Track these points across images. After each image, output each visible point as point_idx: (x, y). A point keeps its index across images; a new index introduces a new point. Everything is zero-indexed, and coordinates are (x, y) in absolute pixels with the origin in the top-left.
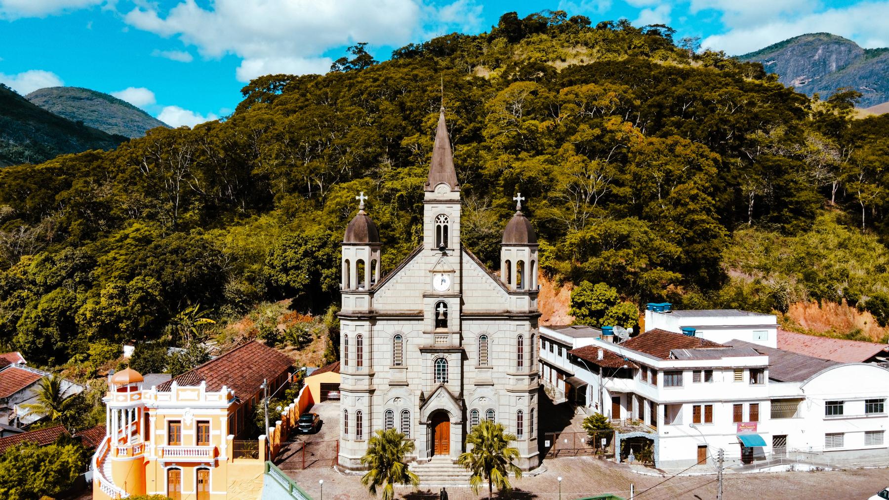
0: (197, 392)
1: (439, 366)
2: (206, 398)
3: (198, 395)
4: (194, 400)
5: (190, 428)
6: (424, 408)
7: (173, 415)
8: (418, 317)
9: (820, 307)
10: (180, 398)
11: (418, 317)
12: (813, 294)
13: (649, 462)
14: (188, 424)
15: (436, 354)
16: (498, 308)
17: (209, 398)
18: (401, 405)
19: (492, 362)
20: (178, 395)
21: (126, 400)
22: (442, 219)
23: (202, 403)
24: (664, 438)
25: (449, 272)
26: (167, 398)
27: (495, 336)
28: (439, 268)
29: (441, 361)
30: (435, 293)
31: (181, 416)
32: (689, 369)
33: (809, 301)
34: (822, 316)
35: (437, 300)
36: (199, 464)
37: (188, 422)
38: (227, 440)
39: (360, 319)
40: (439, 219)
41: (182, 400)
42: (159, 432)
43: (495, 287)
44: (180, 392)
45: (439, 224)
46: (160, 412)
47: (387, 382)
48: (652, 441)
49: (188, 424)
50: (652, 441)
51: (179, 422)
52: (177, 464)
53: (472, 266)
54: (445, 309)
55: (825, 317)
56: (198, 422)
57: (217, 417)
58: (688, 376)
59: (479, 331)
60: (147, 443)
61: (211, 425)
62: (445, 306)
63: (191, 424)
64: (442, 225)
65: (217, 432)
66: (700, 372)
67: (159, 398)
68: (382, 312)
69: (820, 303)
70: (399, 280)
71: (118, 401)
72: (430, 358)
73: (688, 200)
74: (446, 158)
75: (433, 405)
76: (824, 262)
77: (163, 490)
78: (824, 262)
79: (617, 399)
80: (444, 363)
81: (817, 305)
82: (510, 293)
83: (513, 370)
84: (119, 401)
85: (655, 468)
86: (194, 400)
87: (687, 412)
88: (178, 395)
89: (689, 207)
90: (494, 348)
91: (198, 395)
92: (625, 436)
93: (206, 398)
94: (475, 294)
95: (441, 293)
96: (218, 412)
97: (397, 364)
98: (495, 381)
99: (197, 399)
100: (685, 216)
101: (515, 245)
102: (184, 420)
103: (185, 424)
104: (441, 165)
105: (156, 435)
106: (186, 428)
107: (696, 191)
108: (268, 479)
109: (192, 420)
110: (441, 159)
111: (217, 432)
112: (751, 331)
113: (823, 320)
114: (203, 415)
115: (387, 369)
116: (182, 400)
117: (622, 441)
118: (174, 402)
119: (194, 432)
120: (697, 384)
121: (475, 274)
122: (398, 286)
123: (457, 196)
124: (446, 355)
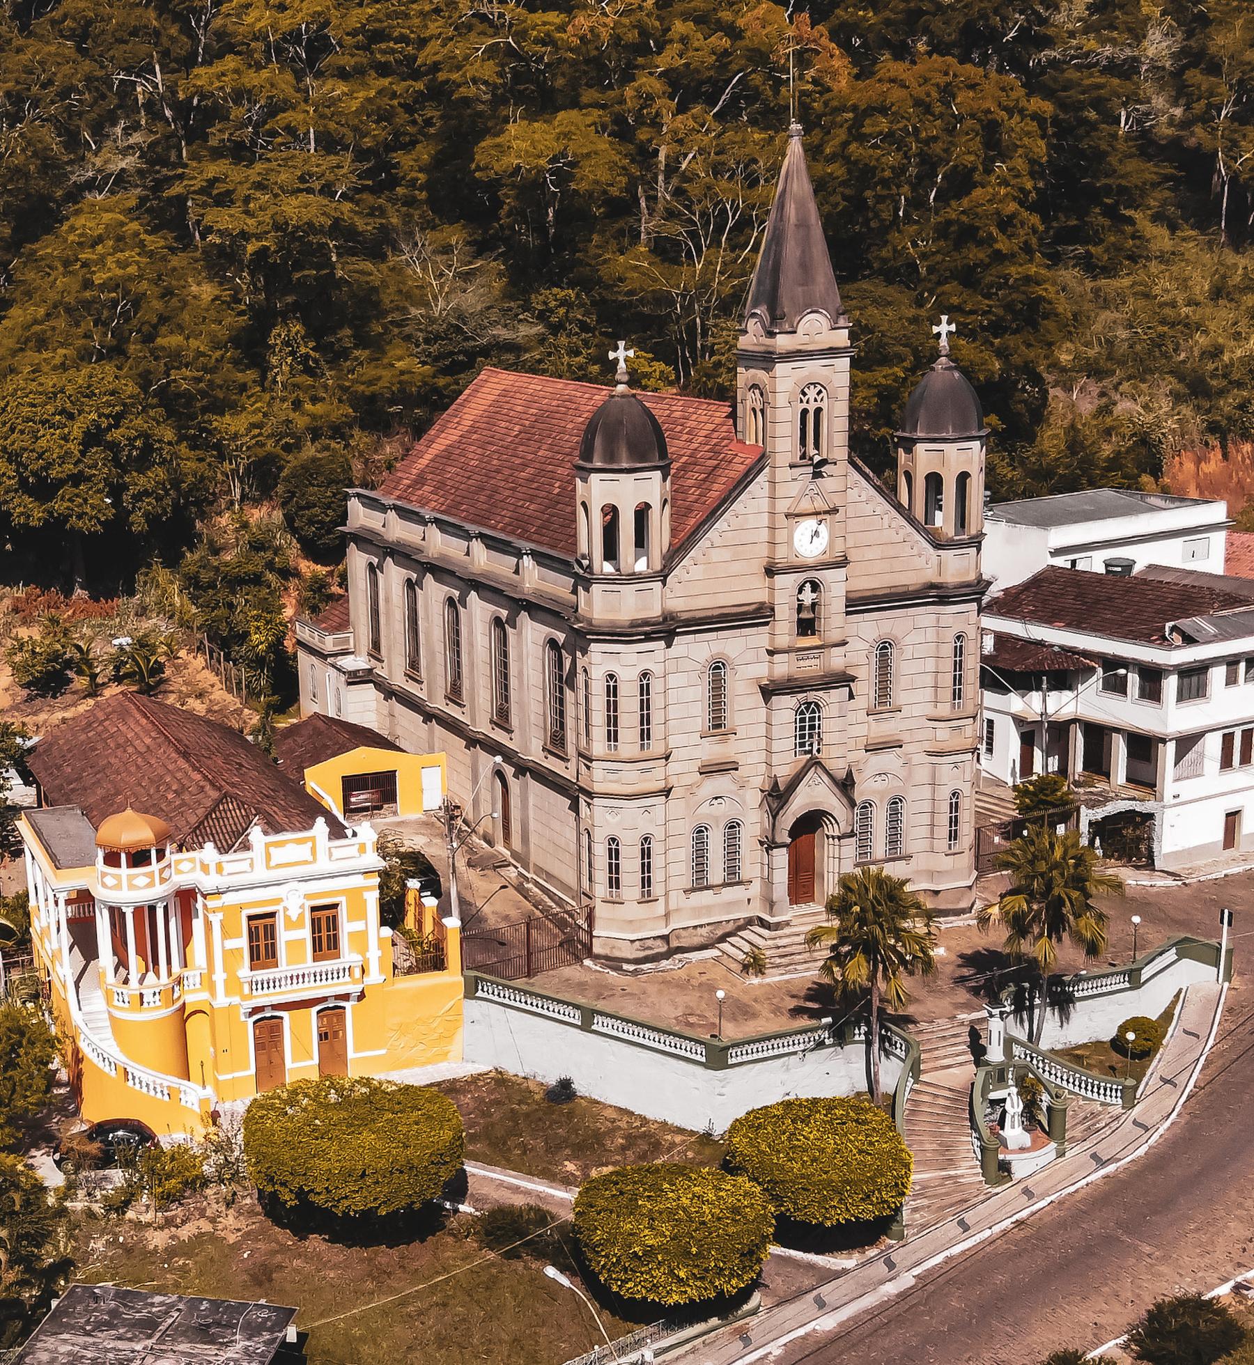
0: (310, 844)
1: (803, 720)
2: (330, 855)
3: (313, 851)
4: (306, 862)
5: (298, 925)
6: (781, 813)
7: (256, 901)
8: (760, 615)
9: (1225, 456)
10: (272, 864)
11: (760, 615)
12: (1213, 428)
13: (1139, 859)
14: (294, 918)
15: (800, 696)
16: (912, 579)
17: (337, 853)
18: (724, 811)
19: (900, 696)
20: (268, 856)
21: (151, 885)
22: (812, 393)
23: (324, 865)
24: (1175, 805)
25: (826, 512)
26: (244, 866)
27: (908, 640)
28: (805, 506)
29: (807, 709)
30: (796, 561)
31: (278, 901)
32: (1215, 661)
33: (1207, 444)
34: (1231, 477)
35: (801, 577)
36: (325, 999)
37: (294, 914)
38: (379, 939)
39: (649, 638)
40: (804, 394)
41: (279, 866)
42: (231, 944)
43: (909, 535)
44: (272, 850)
45: (805, 405)
46: (229, 899)
47: (695, 766)
48: (1151, 816)
49: (294, 918)
50: (1151, 816)
51: (272, 915)
52: (275, 1007)
53: (864, 494)
54: (814, 595)
55: (1235, 479)
56: (314, 909)
57: (355, 895)
58: (1217, 675)
59: (875, 636)
60: (186, 973)
61: (343, 913)
62: (815, 587)
63: (301, 916)
64: (812, 408)
65: (358, 926)
66: (1237, 662)
67: (228, 868)
68: (685, 616)
69: (1224, 447)
70: (718, 541)
71: (132, 887)
72: (786, 705)
73: (994, 231)
74: (814, 250)
75: (798, 805)
76: (1201, 340)
77: (248, 1068)
78: (1201, 340)
79: (1029, 730)
80: (813, 712)
81: (1218, 454)
82: (938, 546)
83: (944, 710)
84: (138, 888)
85: (1154, 870)
86: (306, 862)
87: (1213, 744)
88: (268, 856)
89: (997, 246)
90: (903, 666)
91: (313, 851)
92: (1099, 813)
93: (330, 855)
94: (870, 554)
95: (811, 562)
96: (358, 881)
97: (718, 724)
98: (906, 737)
99: (310, 858)
100: (987, 267)
101: (954, 441)
102: (286, 909)
103: (287, 918)
104: (805, 266)
105: (224, 951)
106: (290, 925)
107: (1012, 207)
108: (474, 1008)
109: (302, 907)
110: (803, 252)
111: (358, 926)
112: (1178, 542)
113: (1232, 485)
114: (324, 890)
115: (695, 738)
116: (279, 866)
117: (1091, 824)
118: (261, 874)
119: (306, 933)
120: (1233, 690)
121: (868, 509)
122: (716, 555)
123: (841, 338)
124: (821, 693)
